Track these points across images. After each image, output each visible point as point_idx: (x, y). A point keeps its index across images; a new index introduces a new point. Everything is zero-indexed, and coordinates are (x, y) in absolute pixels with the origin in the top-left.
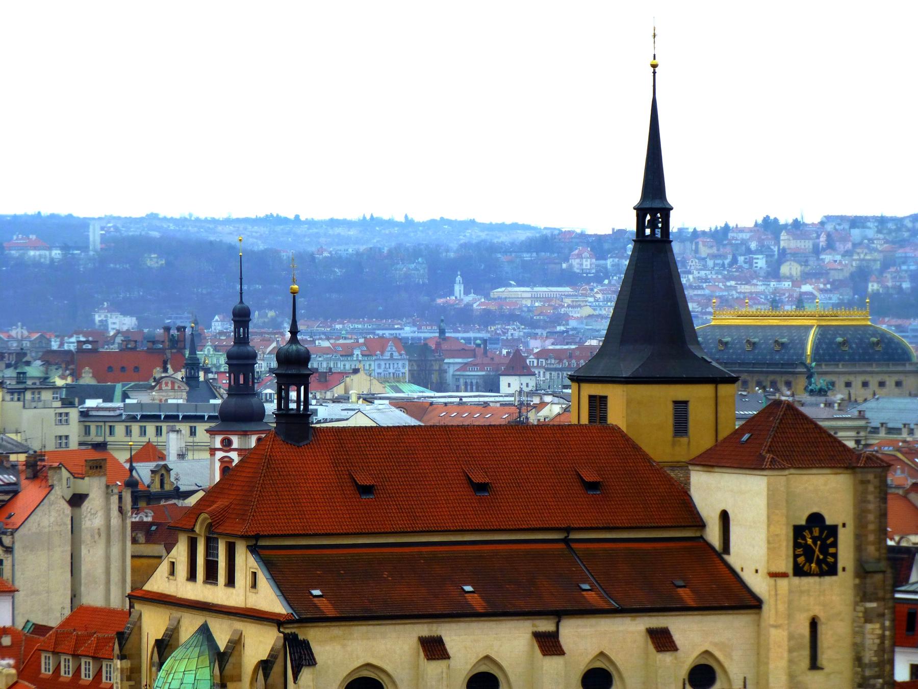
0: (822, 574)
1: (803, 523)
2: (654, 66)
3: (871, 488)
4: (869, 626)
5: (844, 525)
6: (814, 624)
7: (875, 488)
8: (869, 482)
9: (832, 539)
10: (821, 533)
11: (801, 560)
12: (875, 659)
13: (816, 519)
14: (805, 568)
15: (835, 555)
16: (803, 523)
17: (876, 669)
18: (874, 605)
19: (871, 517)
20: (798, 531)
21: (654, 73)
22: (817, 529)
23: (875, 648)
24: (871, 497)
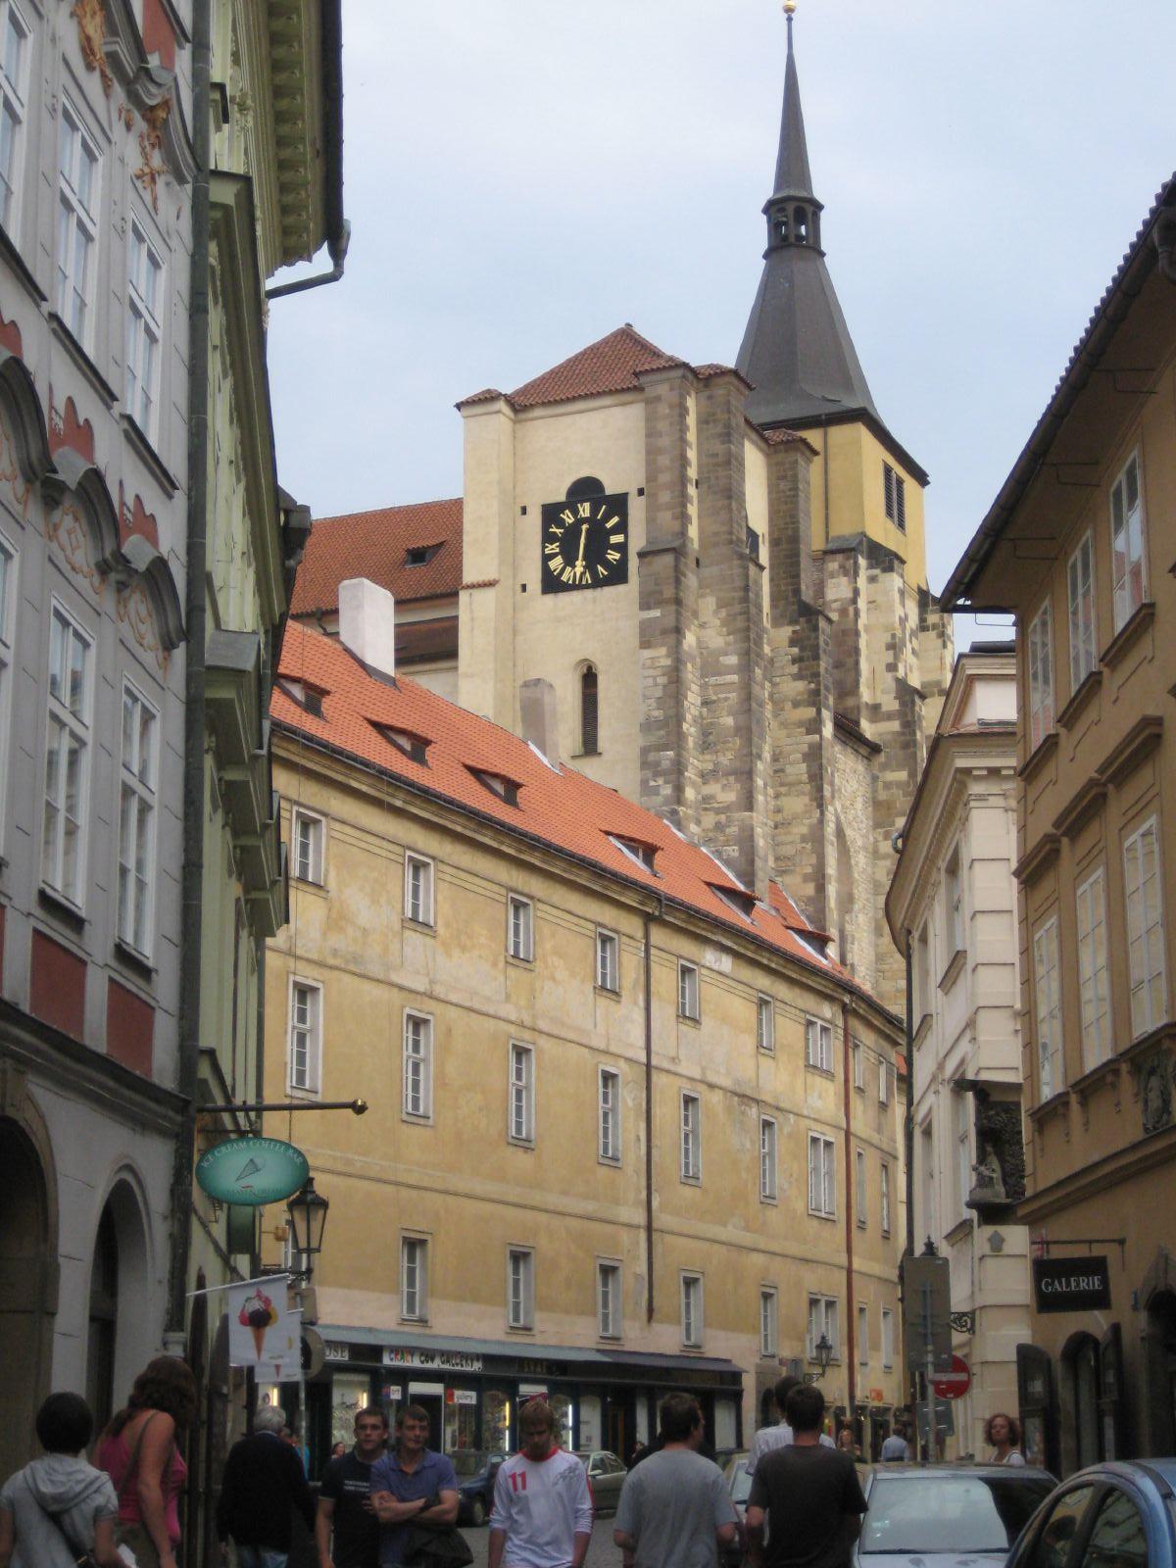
0: (598, 583)
1: (562, 498)
2: (789, 10)
3: (663, 409)
4: (647, 653)
5: (641, 492)
6: (589, 679)
7: (671, 407)
8: (658, 399)
9: (615, 520)
10: (594, 510)
11: (556, 564)
12: (658, 714)
13: (586, 489)
14: (564, 578)
15: (622, 548)
16: (561, 497)
17: (662, 732)
18: (656, 613)
19: (664, 461)
20: (551, 513)
21: (790, 19)
22: (587, 505)
23: (659, 693)
24: (662, 426)
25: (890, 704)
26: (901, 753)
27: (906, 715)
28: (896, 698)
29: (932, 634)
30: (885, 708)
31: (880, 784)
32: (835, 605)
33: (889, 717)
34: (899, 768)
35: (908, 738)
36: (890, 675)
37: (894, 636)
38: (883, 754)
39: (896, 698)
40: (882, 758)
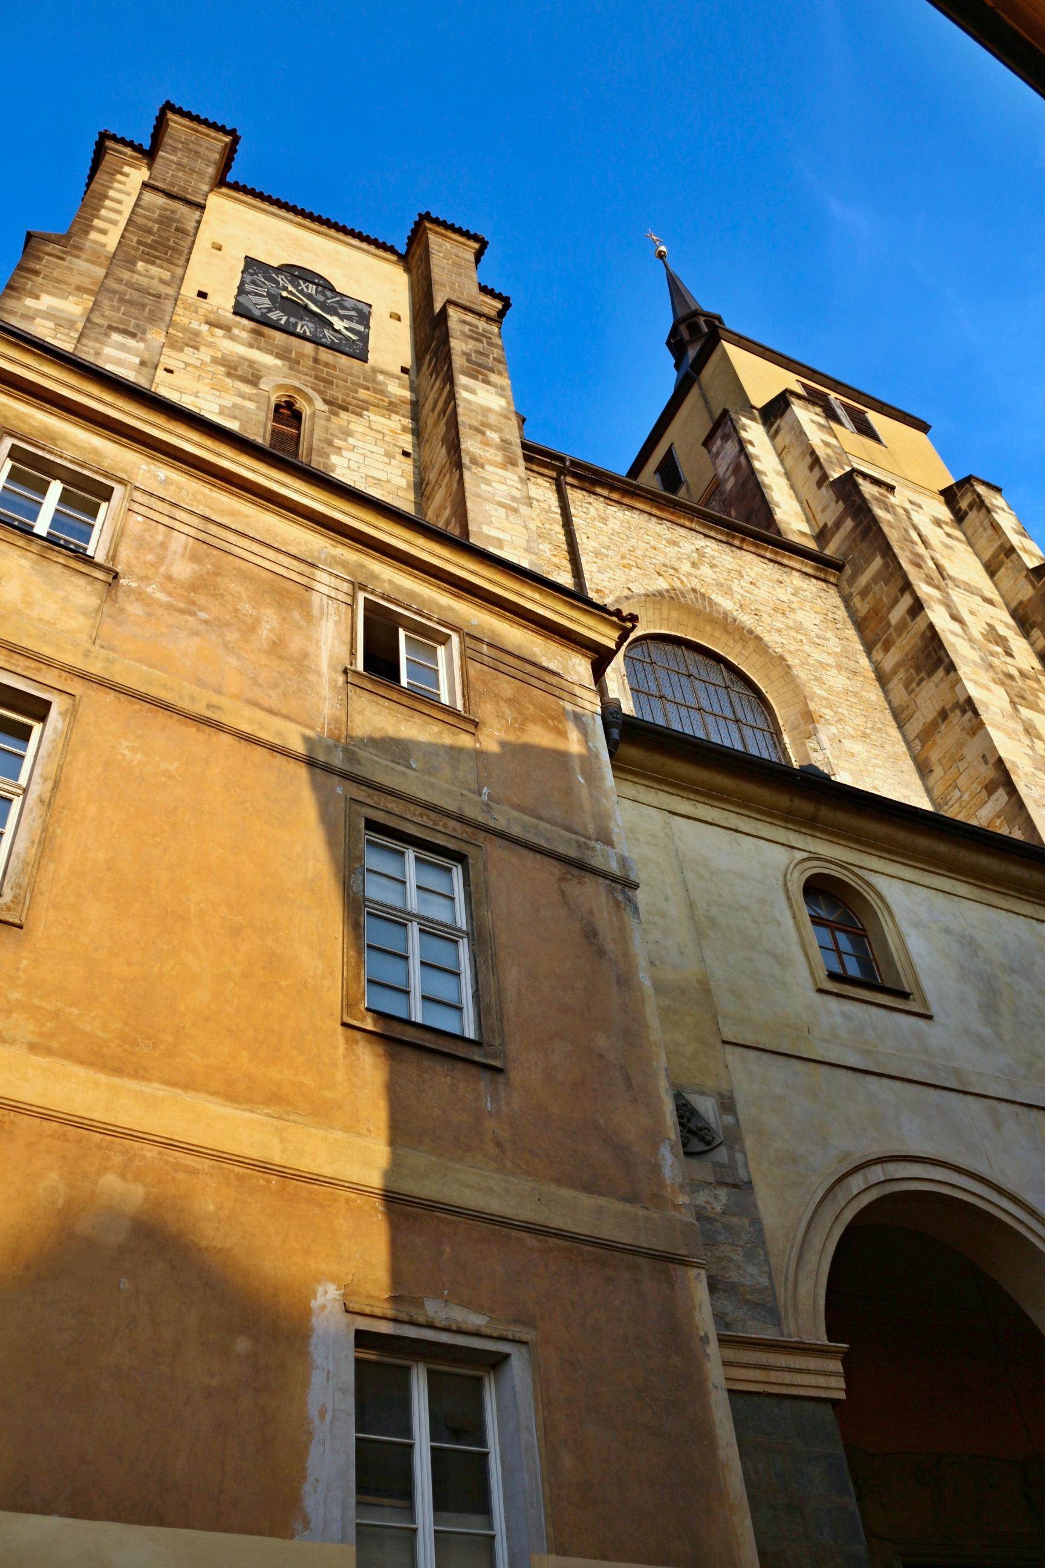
25: (830, 510)
26: (864, 546)
27: (854, 502)
28: (837, 502)
29: (972, 515)
30: (830, 524)
31: (857, 601)
32: (728, 473)
33: (838, 524)
34: (868, 561)
35: (865, 522)
36: (823, 489)
37: (813, 452)
38: (847, 567)
39: (837, 502)
40: (848, 570)
